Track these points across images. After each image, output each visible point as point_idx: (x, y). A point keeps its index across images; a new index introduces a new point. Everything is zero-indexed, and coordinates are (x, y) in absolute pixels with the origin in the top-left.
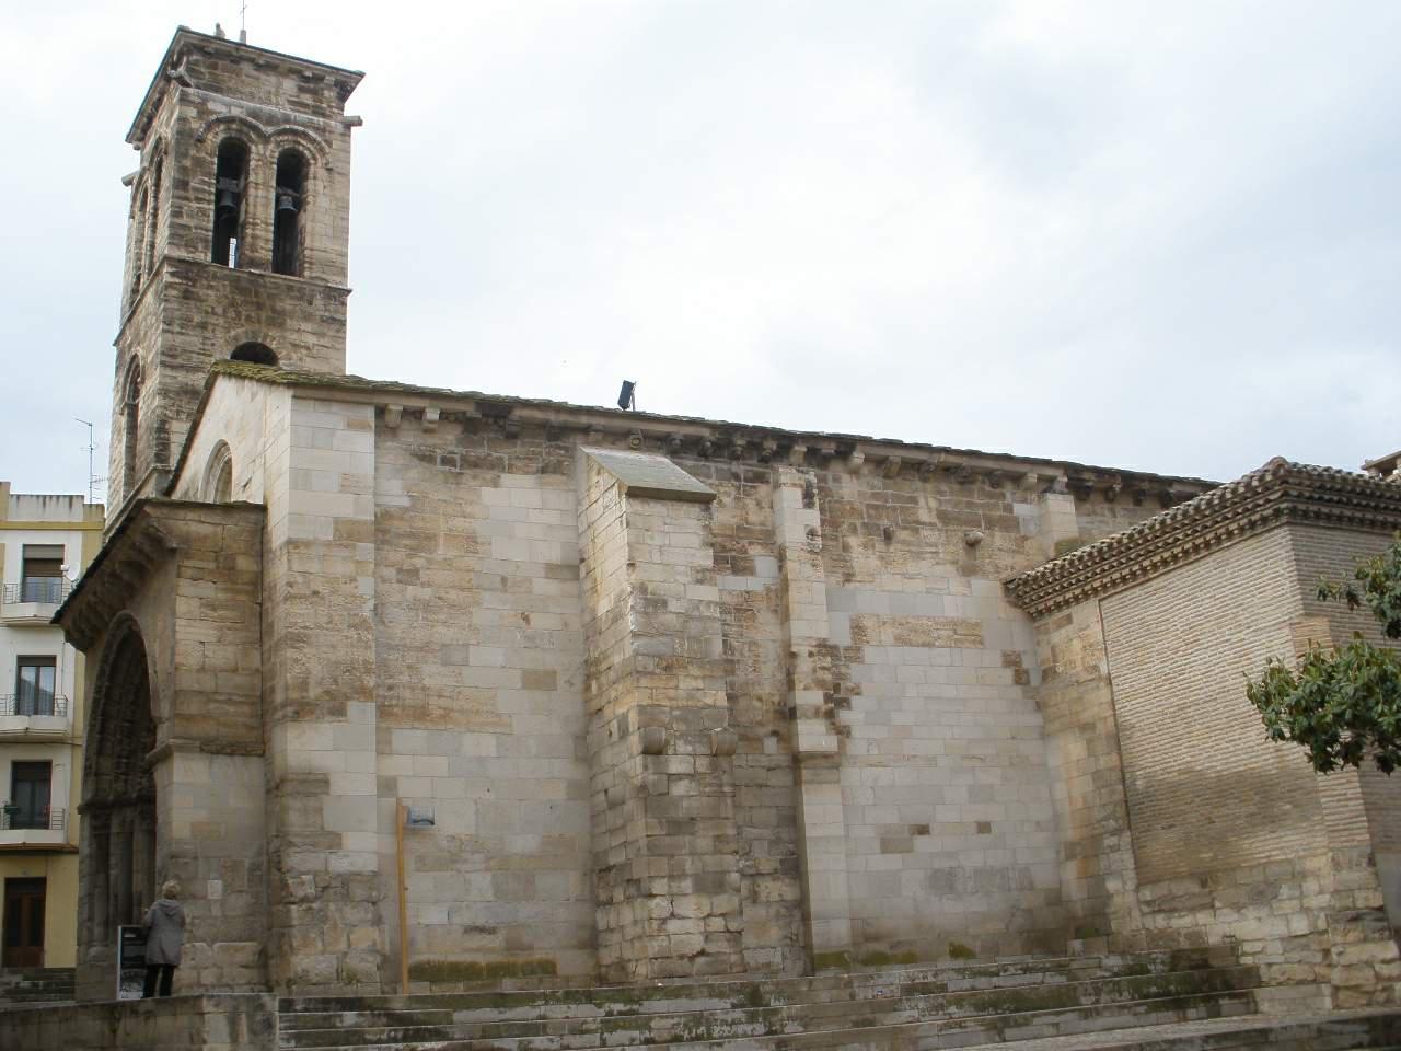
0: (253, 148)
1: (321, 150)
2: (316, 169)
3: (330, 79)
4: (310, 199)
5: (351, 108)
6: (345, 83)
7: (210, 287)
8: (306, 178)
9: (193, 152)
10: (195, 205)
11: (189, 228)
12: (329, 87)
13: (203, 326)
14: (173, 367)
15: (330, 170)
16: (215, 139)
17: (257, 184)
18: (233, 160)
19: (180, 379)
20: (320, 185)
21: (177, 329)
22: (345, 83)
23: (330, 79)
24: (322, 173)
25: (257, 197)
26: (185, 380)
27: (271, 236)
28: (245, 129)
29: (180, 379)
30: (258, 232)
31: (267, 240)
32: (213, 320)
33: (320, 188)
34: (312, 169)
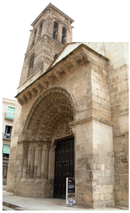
0: (59, 24)
1: (69, 29)
2: (68, 31)
3: (70, 20)
4: (67, 35)
5: (72, 25)
6: (72, 21)
7: (52, 42)
8: (66, 32)
9: (51, 21)
10: (50, 28)
11: (50, 32)
12: (69, 21)
13: (51, 48)
14: (45, 53)
15: (70, 32)
16: (54, 20)
17: (60, 30)
18: (56, 25)
19: (46, 56)
20: (68, 34)
21: (46, 47)
22: (72, 21)
23: (70, 20)
24: (69, 32)
25: (59, 32)
26: (47, 56)
27: (61, 38)
28: (58, 21)
29: (46, 56)
30: (59, 37)
31: (61, 39)
32: (52, 48)
33: (68, 34)
34: (67, 31)
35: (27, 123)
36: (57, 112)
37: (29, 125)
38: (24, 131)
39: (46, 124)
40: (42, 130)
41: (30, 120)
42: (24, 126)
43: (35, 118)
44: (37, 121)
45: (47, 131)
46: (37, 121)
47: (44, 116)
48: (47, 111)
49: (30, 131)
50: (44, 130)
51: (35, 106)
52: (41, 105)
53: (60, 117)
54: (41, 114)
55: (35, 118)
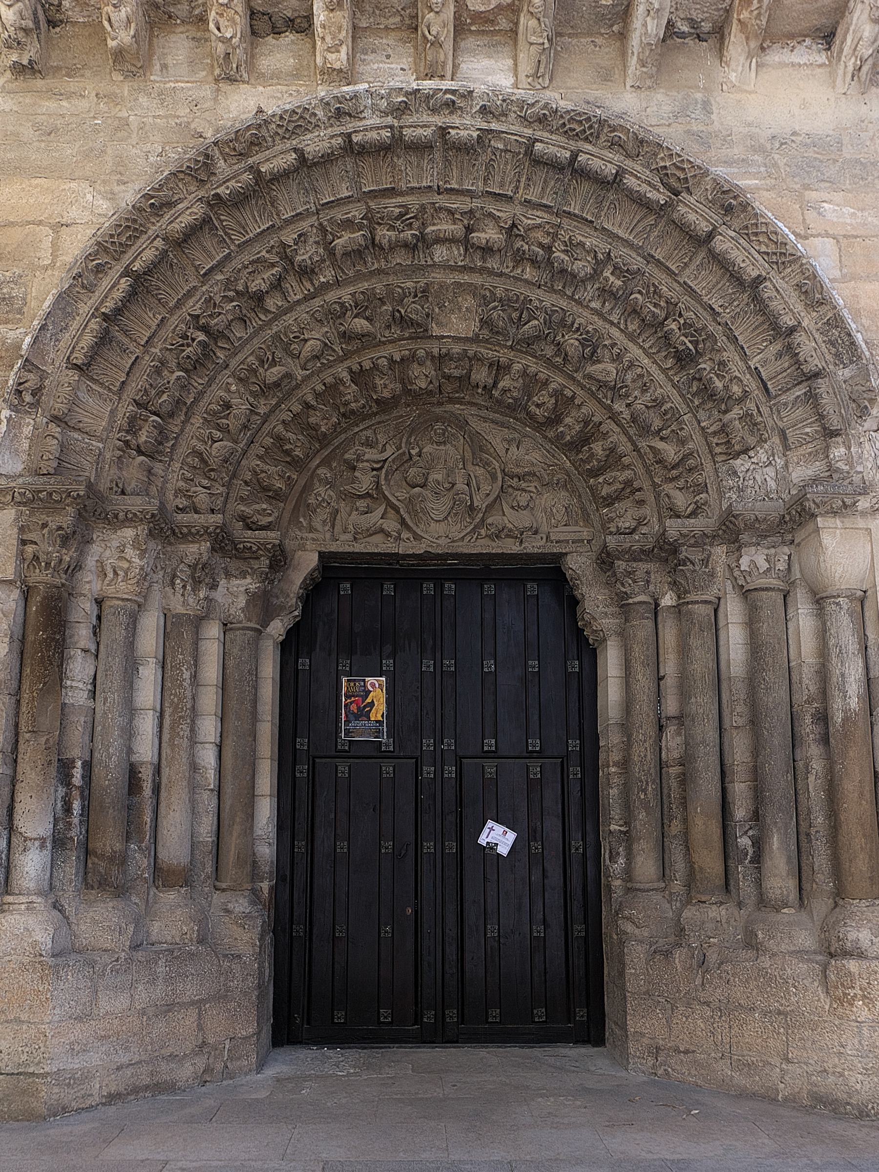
35: (85, 308)
36: (418, 330)
37: (104, 340)
38: (32, 380)
39: (266, 389)
40: (218, 434)
41: (132, 295)
42: (43, 328)
43: (189, 294)
44: (201, 337)
45: (260, 457)
46: (205, 329)
47: (275, 319)
48: (326, 276)
49: (100, 413)
50: (236, 442)
51: (230, 178)
52: (291, 201)
53: (422, 377)
54: (258, 284)
55: (189, 294)
